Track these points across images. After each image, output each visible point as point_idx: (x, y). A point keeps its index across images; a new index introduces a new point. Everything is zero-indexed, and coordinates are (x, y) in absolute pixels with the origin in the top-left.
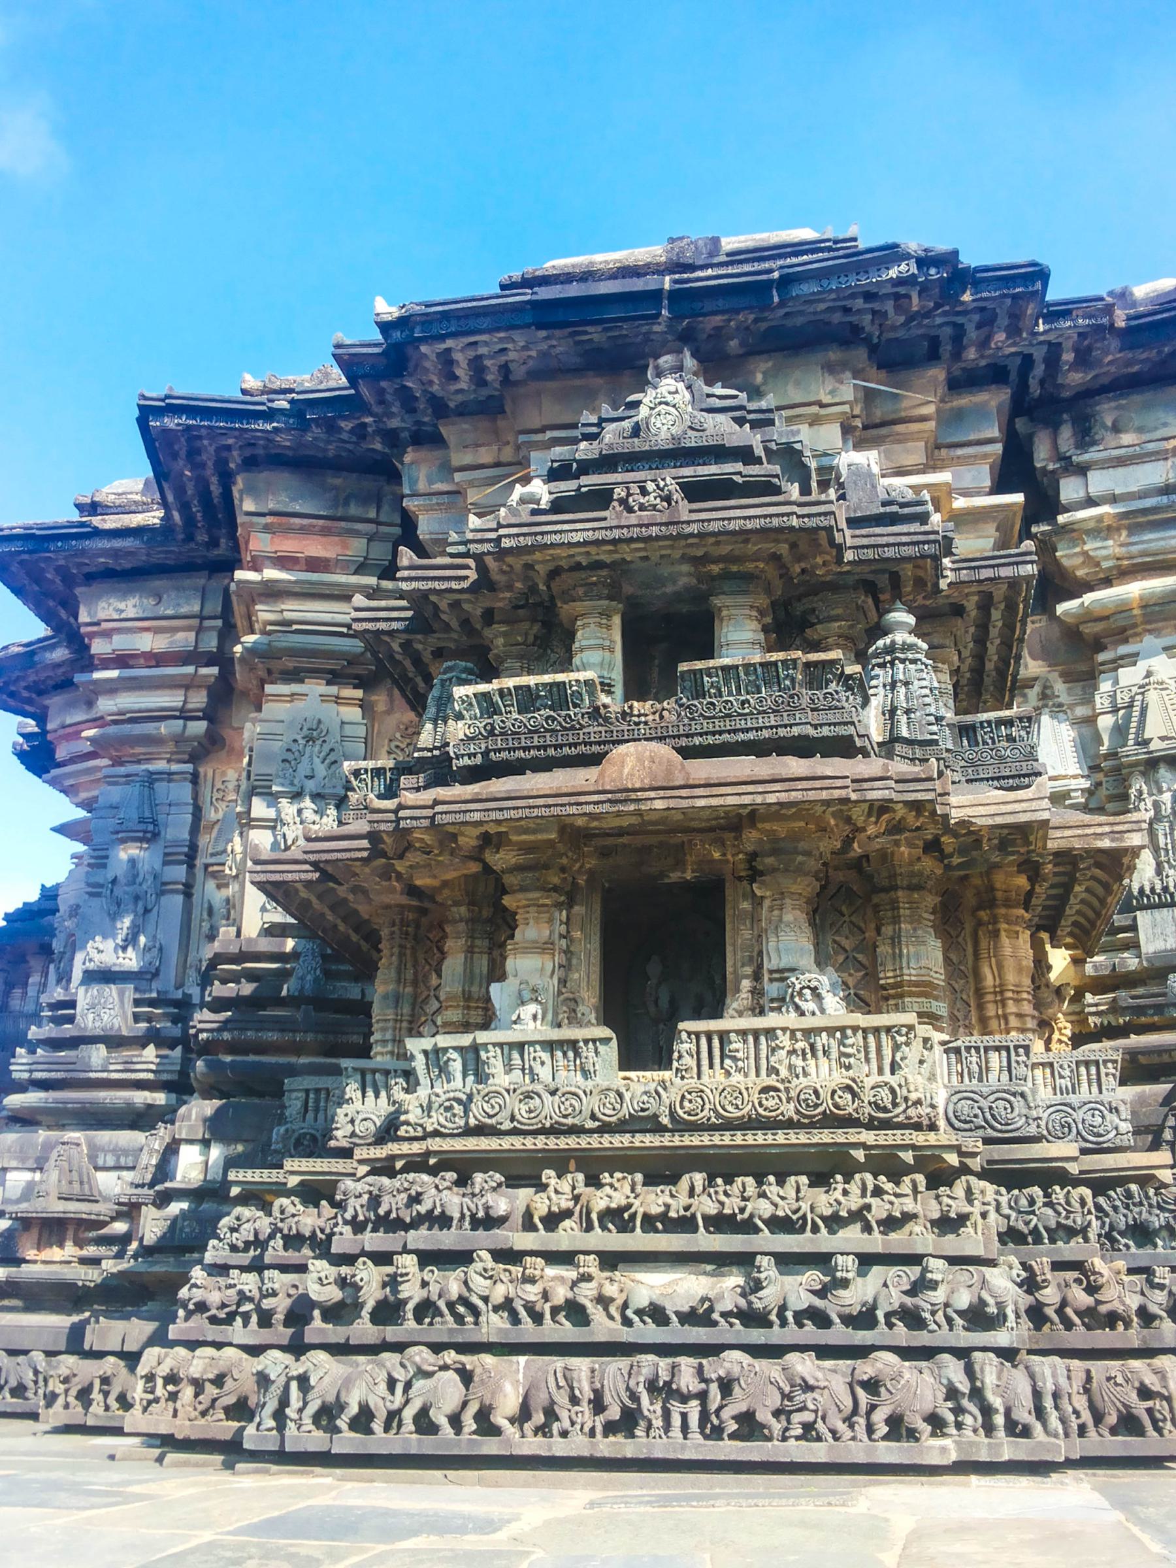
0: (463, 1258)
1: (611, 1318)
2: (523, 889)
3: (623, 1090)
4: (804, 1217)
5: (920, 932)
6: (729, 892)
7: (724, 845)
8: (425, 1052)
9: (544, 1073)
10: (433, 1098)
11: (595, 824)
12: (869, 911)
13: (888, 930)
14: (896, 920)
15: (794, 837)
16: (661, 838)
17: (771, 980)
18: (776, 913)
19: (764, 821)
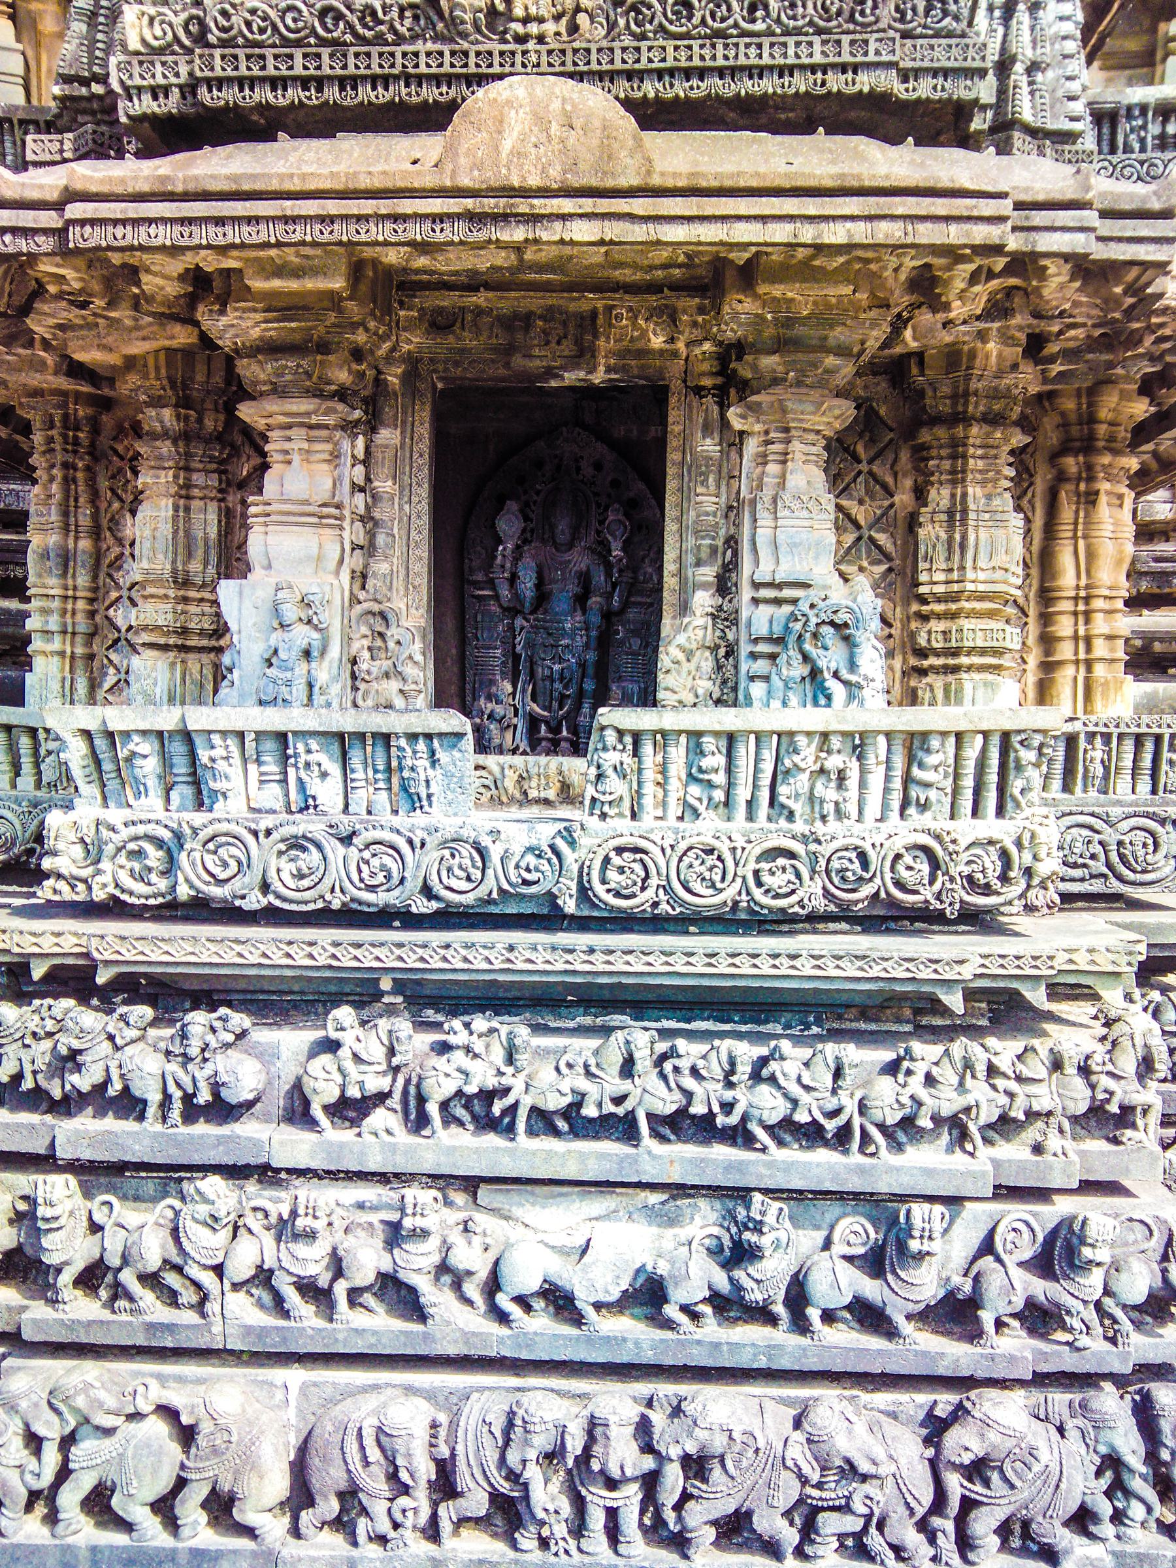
0: (172, 1175)
1: (469, 1302)
2: (278, 391)
3: (486, 841)
4: (848, 1126)
5: (996, 502)
6: (674, 415)
7: (673, 319)
8: (87, 734)
9: (328, 793)
10: (105, 834)
11: (422, 262)
12: (905, 456)
13: (940, 497)
14: (957, 477)
15: (826, 316)
16: (552, 300)
17: (756, 601)
18: (773, 468)
19: (774, 279)
